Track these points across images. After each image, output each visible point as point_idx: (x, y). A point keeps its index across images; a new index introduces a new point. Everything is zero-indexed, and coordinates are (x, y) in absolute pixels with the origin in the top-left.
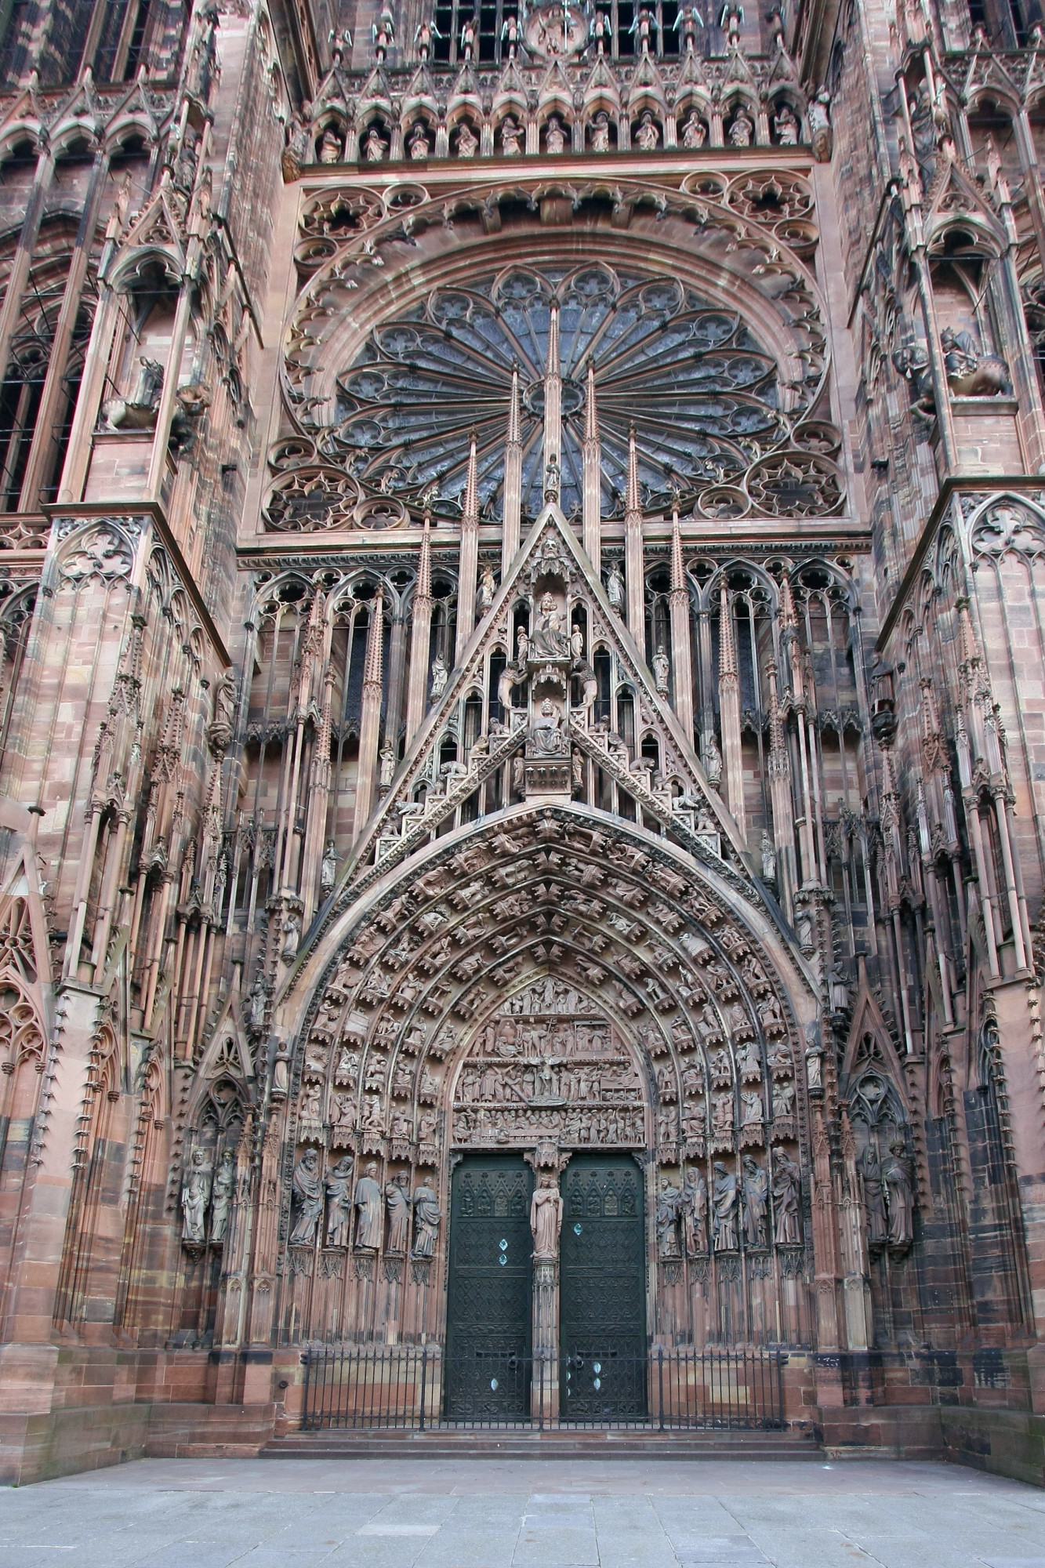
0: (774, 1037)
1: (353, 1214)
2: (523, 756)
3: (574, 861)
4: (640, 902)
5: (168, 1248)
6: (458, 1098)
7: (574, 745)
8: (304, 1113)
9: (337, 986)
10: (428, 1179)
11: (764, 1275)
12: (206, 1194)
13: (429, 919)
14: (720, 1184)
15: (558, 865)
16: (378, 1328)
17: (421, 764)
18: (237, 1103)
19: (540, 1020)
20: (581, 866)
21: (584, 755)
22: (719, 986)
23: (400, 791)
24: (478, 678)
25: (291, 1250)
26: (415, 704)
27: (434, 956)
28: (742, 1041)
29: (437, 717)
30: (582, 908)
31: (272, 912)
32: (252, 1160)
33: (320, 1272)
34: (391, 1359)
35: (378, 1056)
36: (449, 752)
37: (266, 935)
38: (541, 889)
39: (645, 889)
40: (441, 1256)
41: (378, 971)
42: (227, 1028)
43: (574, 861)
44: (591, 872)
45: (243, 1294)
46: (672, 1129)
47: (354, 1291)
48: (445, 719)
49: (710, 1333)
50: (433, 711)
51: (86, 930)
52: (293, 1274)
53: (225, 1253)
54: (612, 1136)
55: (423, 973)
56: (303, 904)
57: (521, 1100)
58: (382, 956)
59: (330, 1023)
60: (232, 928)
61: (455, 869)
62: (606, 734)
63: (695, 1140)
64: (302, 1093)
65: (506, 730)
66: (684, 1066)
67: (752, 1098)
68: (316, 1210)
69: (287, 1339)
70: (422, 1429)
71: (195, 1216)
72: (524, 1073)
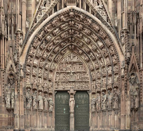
0: (115, 65)
1: (38, 103)
3: (77, 23)
5: (4, 109)
8: (27, 81)
9: (31, 52)
10: (51, 96)
11: (111, 115)
13: (48, 37)
14: (104, 97)
15: (74, 24)
16: (43, 125)
18: (14, 79)
20: (78, 25)
22: (105, 54)
27: (50, 47)
28: (109, 66)
33: (32, 114)
35: (40, 69)
39: (91, 30)
40: (54, 111)
41: (39, 49)
42: (11, 62)
43: (77, 23)
44: (80, 26)
45: (18, 118)
47: (39, 118)
49: (101, 126)
52: (27, 115)
53: (14, 110)
54: (83, 87)
55: (48, 51)
57: (67, 80)
58: (40, 46)
59: (31, 61)
60: (9, 39)
61: (53, 25)
63: (99, 88)
64: (26, 77)
66: (97, 72)
67: (110, 78)
68: (31, 101)
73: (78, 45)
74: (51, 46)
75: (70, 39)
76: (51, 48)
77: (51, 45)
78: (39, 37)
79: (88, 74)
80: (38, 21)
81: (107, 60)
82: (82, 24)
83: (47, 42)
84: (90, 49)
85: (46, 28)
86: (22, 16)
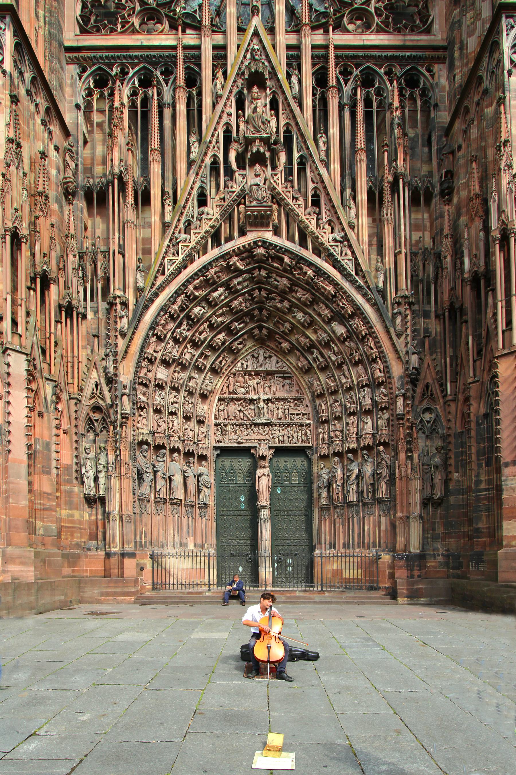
2: (244, 204)
4: (310, 302)
6: (216, 418)
7: (273, 197)
12: (94, 470)
13: (196, 310)
17: (187, 208)
19: (257, 374)
21: (279, 205)
23: (176, 227)
24: (216, 149)
25: (139, 500)
26: (182, 166)
27: (200, 334)
29: (194, 176)
30: (279, 305)
31: (111, 305)
32: (116, 452)
34: (193, 556)
36: (202, 202)
37: (109, 319)
38: (256, 293)
46: (326, 437)
48: (199, 177)
50: (192, 171)
51: (13, 313)
55: (195, 345)
56: (128, 299)
61: (210, 279)
62: (291, 190)
65: (235, 186)
66: (332, 401)
69: (141, 545)
70: (209, 590)
71: (89, 482)
72: (249, 404)
73: (279, 328)
74: (203, 332)
75: (256, 312)
76: (202, 337)
77: (204, 329)
78: (173, 312)
79: (308, 404)
80: (169, 270)
81: (358, 372)
82: (287, 278)
83: (194, 322)
84: (311, 340)
85: (191, 287)
86: (124, 256)
